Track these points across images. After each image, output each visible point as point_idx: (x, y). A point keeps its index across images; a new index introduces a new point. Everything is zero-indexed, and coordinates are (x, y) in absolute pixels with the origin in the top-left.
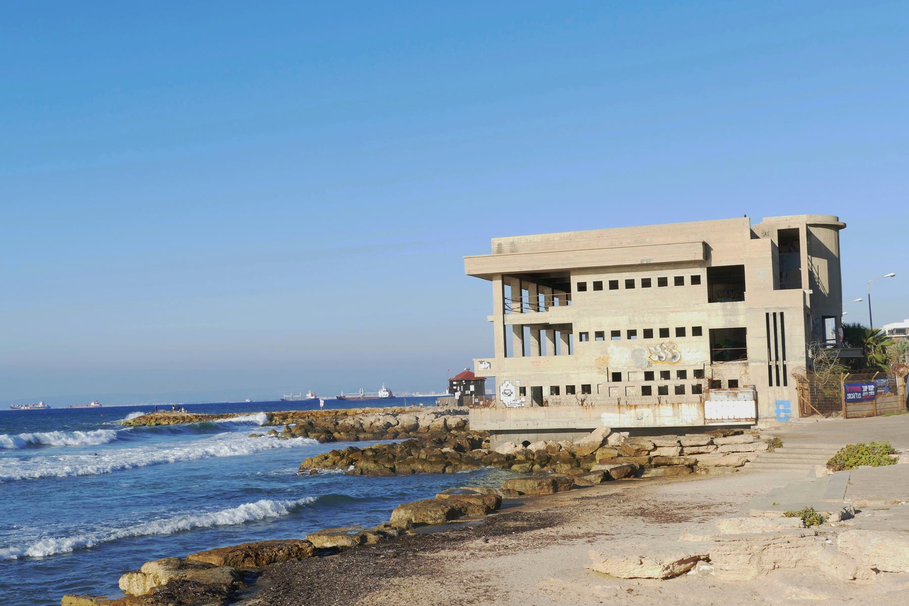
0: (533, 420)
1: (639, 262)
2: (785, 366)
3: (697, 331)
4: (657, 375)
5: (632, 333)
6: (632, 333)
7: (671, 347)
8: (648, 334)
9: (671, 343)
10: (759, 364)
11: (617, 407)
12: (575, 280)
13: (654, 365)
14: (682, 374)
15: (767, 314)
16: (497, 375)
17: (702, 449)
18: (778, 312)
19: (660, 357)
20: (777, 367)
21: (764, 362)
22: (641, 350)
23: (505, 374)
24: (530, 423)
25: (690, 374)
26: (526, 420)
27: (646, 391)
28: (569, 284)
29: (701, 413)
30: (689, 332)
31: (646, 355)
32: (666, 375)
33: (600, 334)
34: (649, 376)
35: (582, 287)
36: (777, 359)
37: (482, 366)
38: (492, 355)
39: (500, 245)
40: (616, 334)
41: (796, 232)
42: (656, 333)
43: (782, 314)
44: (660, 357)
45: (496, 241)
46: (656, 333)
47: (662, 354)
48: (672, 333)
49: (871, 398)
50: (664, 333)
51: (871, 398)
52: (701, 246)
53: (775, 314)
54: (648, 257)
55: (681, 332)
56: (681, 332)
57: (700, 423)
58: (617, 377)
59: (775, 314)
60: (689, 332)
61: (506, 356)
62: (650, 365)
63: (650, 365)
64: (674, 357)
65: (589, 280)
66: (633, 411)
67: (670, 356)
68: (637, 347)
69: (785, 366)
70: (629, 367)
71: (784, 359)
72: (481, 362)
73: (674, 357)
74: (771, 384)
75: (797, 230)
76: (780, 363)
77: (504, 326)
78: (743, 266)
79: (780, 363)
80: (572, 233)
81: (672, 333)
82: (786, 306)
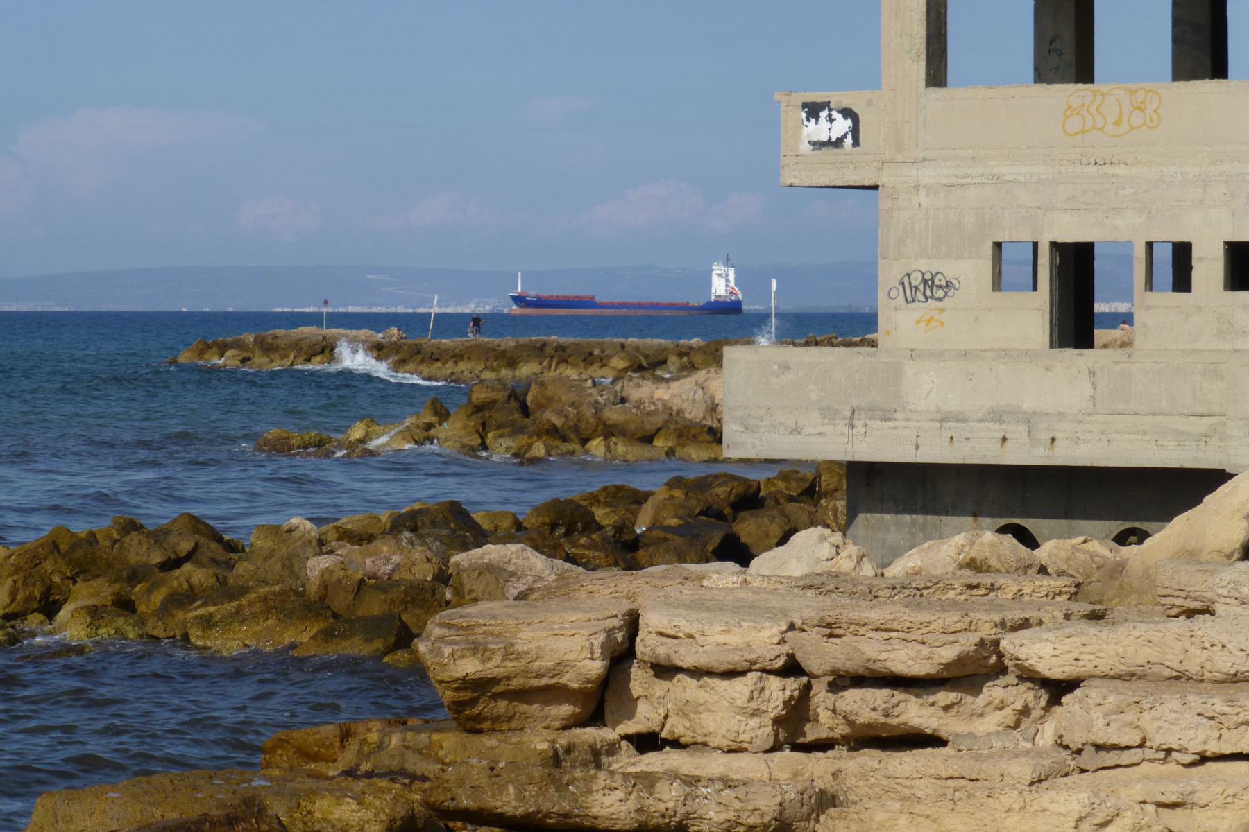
0: (1029, 419)
16: (885, 178)
17: (916, 712)
23: (927, 175)
24: (1018, 432)
26: (996, 416)
37: (821, 130)
49: (940, 299)
51: (940, 299)
61: (937, 75)
72: (813, 110)
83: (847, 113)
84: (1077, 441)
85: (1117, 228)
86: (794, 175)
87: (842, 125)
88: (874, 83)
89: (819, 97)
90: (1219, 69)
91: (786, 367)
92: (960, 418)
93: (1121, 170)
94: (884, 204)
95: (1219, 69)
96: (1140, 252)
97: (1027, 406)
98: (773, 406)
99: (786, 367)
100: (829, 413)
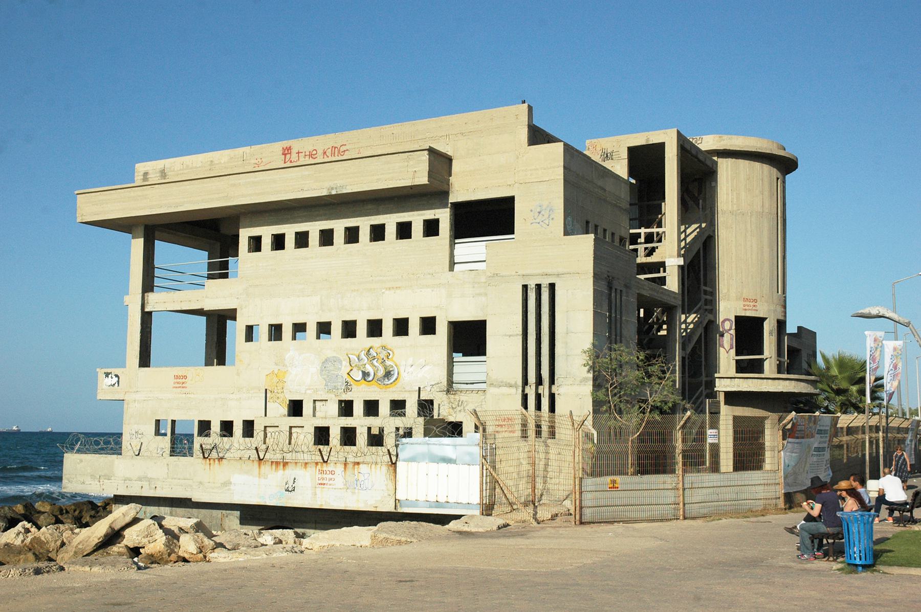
0: (149, 480)
1: (324, 193)
2: (552, 397)
3: (428, 326)
4: (358, 408)
5: (324, 328)
6: (324, 328)
7: (383, 355)
8: (349, 329)
9: (384, 348)
10: (505, 390)
11: (256, 464)
12: (245, 234)
13: (354, 387)
14: (398, 406)
15: (525, 287)
18: (545, 283)
19: (365, 375)
20: (538, 397)
21: (516, 386)
22: (336, 360)
24: (145, 484)
25: (412, 408)
26: (140, 479)
27: (322, 436)
28: (236, 238)
29: (392, 488)
30: (414, 327)
31: (345, 368)
32: (371, 408)
33: (276, 332)
34: (346, 408)
35: (256, 244)
36: (539, 381)
38: (123, 365)
39: (146, 174)
40: (299, 328)
41: (659, 148)
42: (362, 329)
43: (552, 287)
44: (365, 375)
45: (141, 168)
46: (362, 329)
47: (369, 369)
48: (388, 328)
50: (375, 328)
52: (425, 156)
53: (539, 287)
54: (339, 182)
55: (401, 327)
56: (401, 327)
57: (388, 507)
58: (296, 408)
59: (539, 287)
60: (414, 327)
62: (348, 388)
63: (348, 388)
64: (388, 374)
65: (266, 232)
66: (281, 471)
67: (382, 372)
68: (330, 354)
69: (552, 397)
70: (316, 391)
71: (552, 381)
72: (107, 375)
73: (388, 374)
74: (525, 436)
75: (661, 147)
76: (544, 390)
77: (147, 318)
78: (510, 200)
79: (544, 390)
80: (247, 149)
81: (388, 328)
82: (561, 270)
83: (117, 376)
84: (162, 488)
85: (188, 415)
86: (101, 396)
87: (116, 379)
88: (123, 365)
89: (109, 370)
90: (222, 361)
91: (81, 461)
92: (130, 480)
93: (192, 396)
94: (125, 406)
95: (222, 361)
96: (196, 424)
97: (149, 476)
98: (83, 474)
99: (81, 461)
100: (93, 477)
